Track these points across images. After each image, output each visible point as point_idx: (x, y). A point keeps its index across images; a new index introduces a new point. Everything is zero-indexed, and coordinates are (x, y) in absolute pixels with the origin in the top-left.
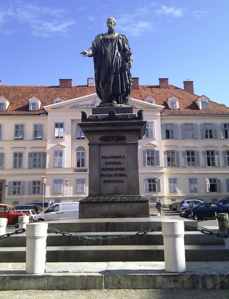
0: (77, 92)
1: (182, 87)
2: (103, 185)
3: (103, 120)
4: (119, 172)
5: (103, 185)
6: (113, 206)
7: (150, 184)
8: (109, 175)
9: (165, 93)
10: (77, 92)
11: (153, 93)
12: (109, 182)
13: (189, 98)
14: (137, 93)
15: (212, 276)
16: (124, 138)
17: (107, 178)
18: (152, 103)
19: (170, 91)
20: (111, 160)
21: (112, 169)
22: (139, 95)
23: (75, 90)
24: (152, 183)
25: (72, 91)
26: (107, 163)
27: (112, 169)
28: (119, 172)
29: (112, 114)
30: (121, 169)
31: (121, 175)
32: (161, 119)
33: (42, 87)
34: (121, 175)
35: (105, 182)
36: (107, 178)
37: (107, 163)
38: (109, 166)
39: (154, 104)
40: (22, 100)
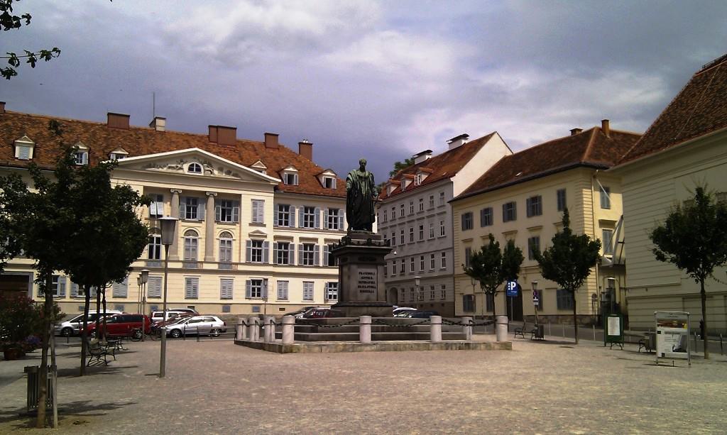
0: (140, 138)
1: (296, 149)
2: (359, 294)
3: (362, 245)
4: (370, 285)
5: (359, 294)
6: (370, 309)
7: (254, 286)
8: (363, 287)
9: (275, 157)
10: (140, 138)
11: (257, 155)
12: (364, 291)
13: (307, 168)
14: (234, 151)
15: (455, 344)
16: (375, 260)
17: (362, 289)
18: (261, 172)
19: (281, 153)
20: (366, 276)
21: (365, 282)
22: (237, 155)
23: (136, 134)
24: (256, 286)
25: (131, 135)
26: (362, 278)
27: (365, 282)
28: (370, 285)
29: (369, 240)
30: (372, 283)
31: (372, 287)
32: (274, 197)
33: (78, 122)
34: (372, 287)
35: (361, 291)
36: (362, 289)
37: (362, 278)
38: (364, 280)
39: (264, 175)
40: (52, 143)
